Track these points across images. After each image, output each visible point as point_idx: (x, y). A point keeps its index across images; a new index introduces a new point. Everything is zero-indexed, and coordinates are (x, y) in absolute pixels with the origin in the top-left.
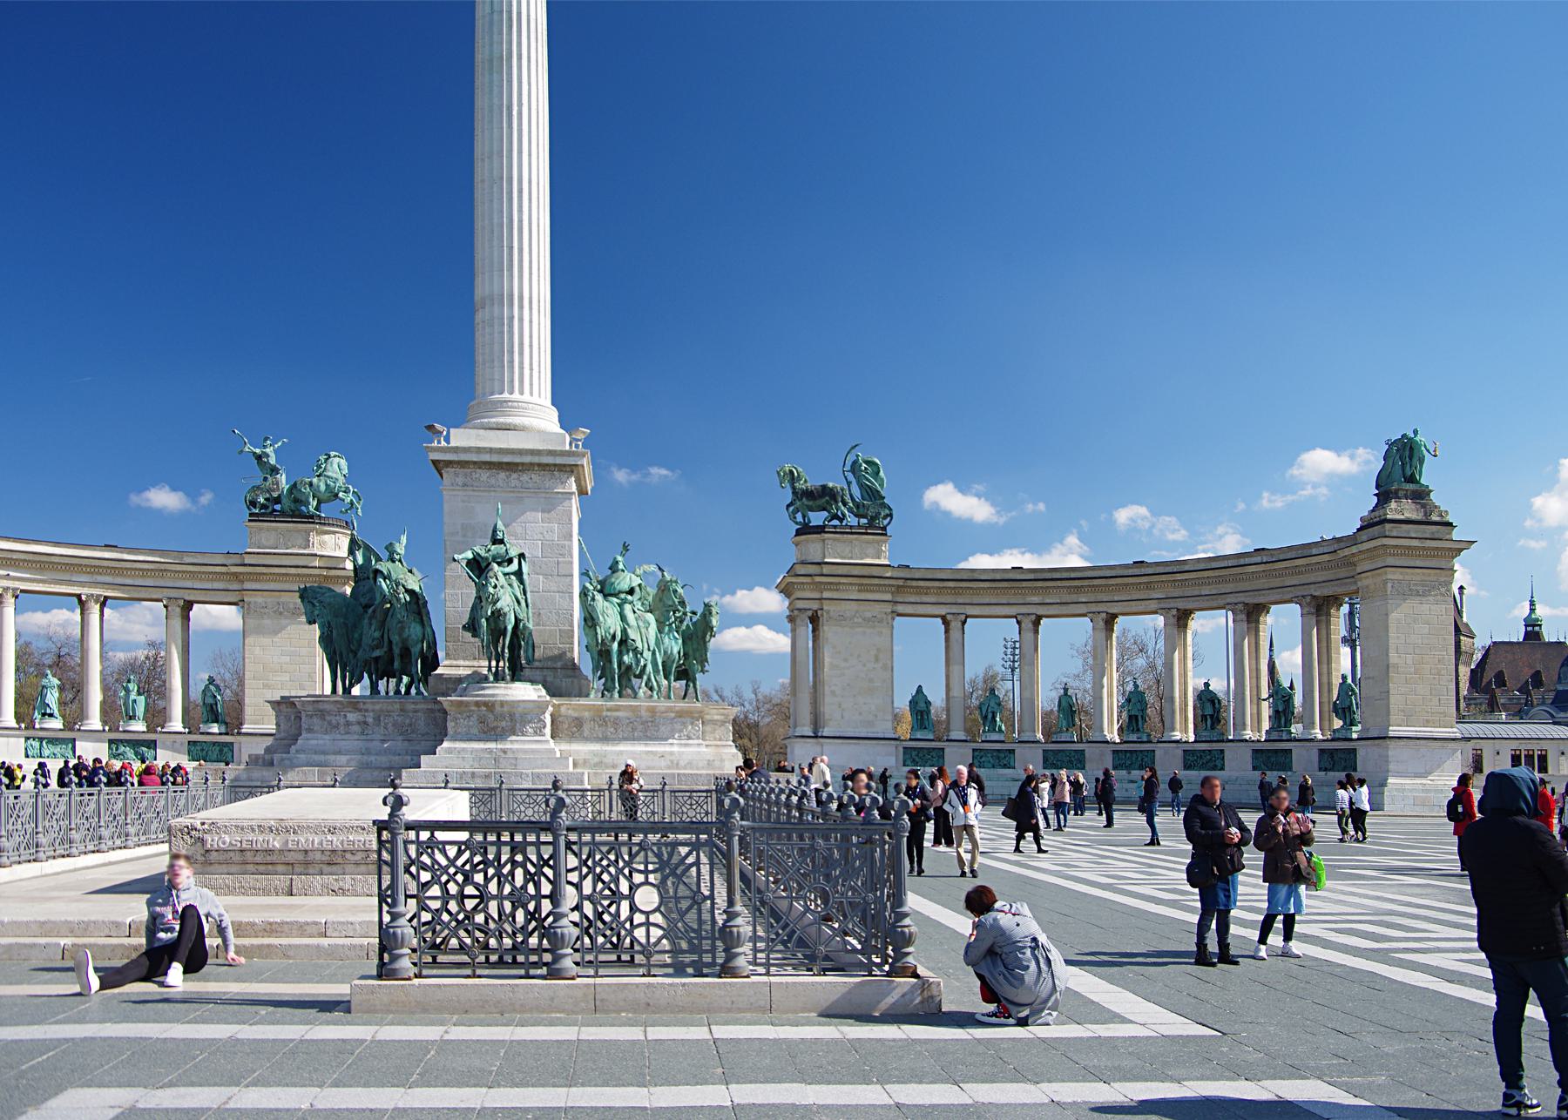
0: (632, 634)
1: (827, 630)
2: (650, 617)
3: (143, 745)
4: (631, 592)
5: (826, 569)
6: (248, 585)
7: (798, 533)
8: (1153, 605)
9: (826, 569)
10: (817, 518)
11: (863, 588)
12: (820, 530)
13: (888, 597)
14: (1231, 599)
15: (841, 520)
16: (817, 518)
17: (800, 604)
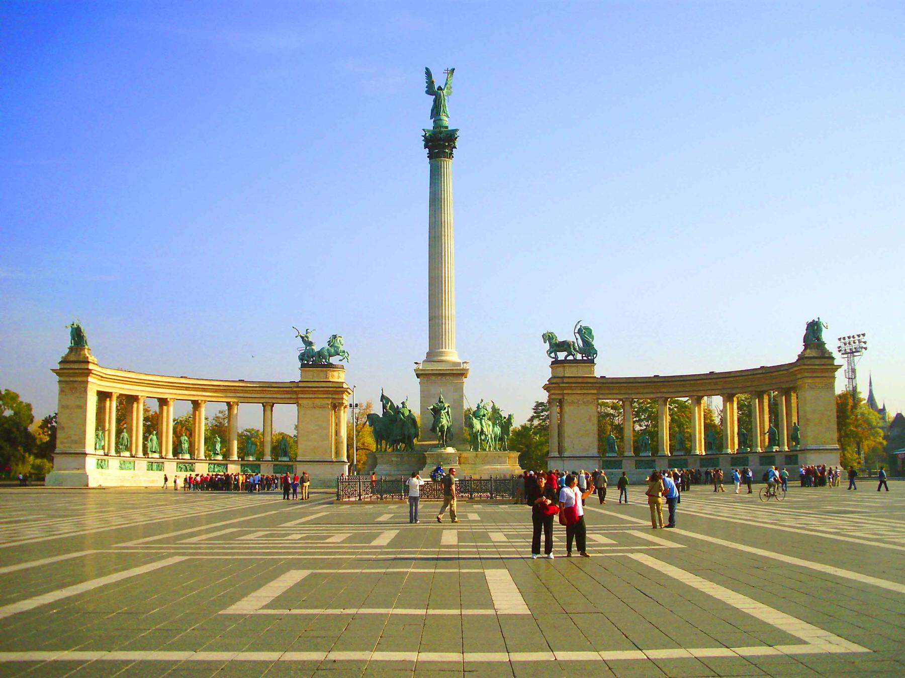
0: (485, 429)
1: (567, 409)
2: (490, 423)
3: (256, 468)
4: (484, 416)
5: (565, 380)
6: (300, 396)
7: (553, 363)
8: (717, 392)
9: (565, 380)
10: (561, 356)
11: (582, 388)
12: (562, 362)
13: (595, 392)
14: (750, 389)
15: (573, 355)
16: (561, 356)
17: (553, 397)
